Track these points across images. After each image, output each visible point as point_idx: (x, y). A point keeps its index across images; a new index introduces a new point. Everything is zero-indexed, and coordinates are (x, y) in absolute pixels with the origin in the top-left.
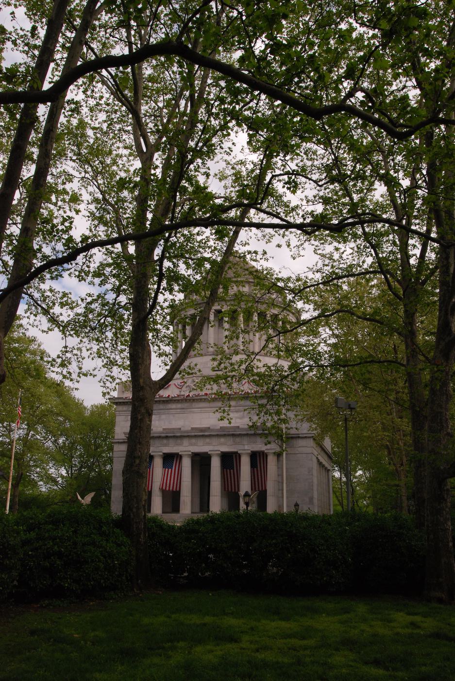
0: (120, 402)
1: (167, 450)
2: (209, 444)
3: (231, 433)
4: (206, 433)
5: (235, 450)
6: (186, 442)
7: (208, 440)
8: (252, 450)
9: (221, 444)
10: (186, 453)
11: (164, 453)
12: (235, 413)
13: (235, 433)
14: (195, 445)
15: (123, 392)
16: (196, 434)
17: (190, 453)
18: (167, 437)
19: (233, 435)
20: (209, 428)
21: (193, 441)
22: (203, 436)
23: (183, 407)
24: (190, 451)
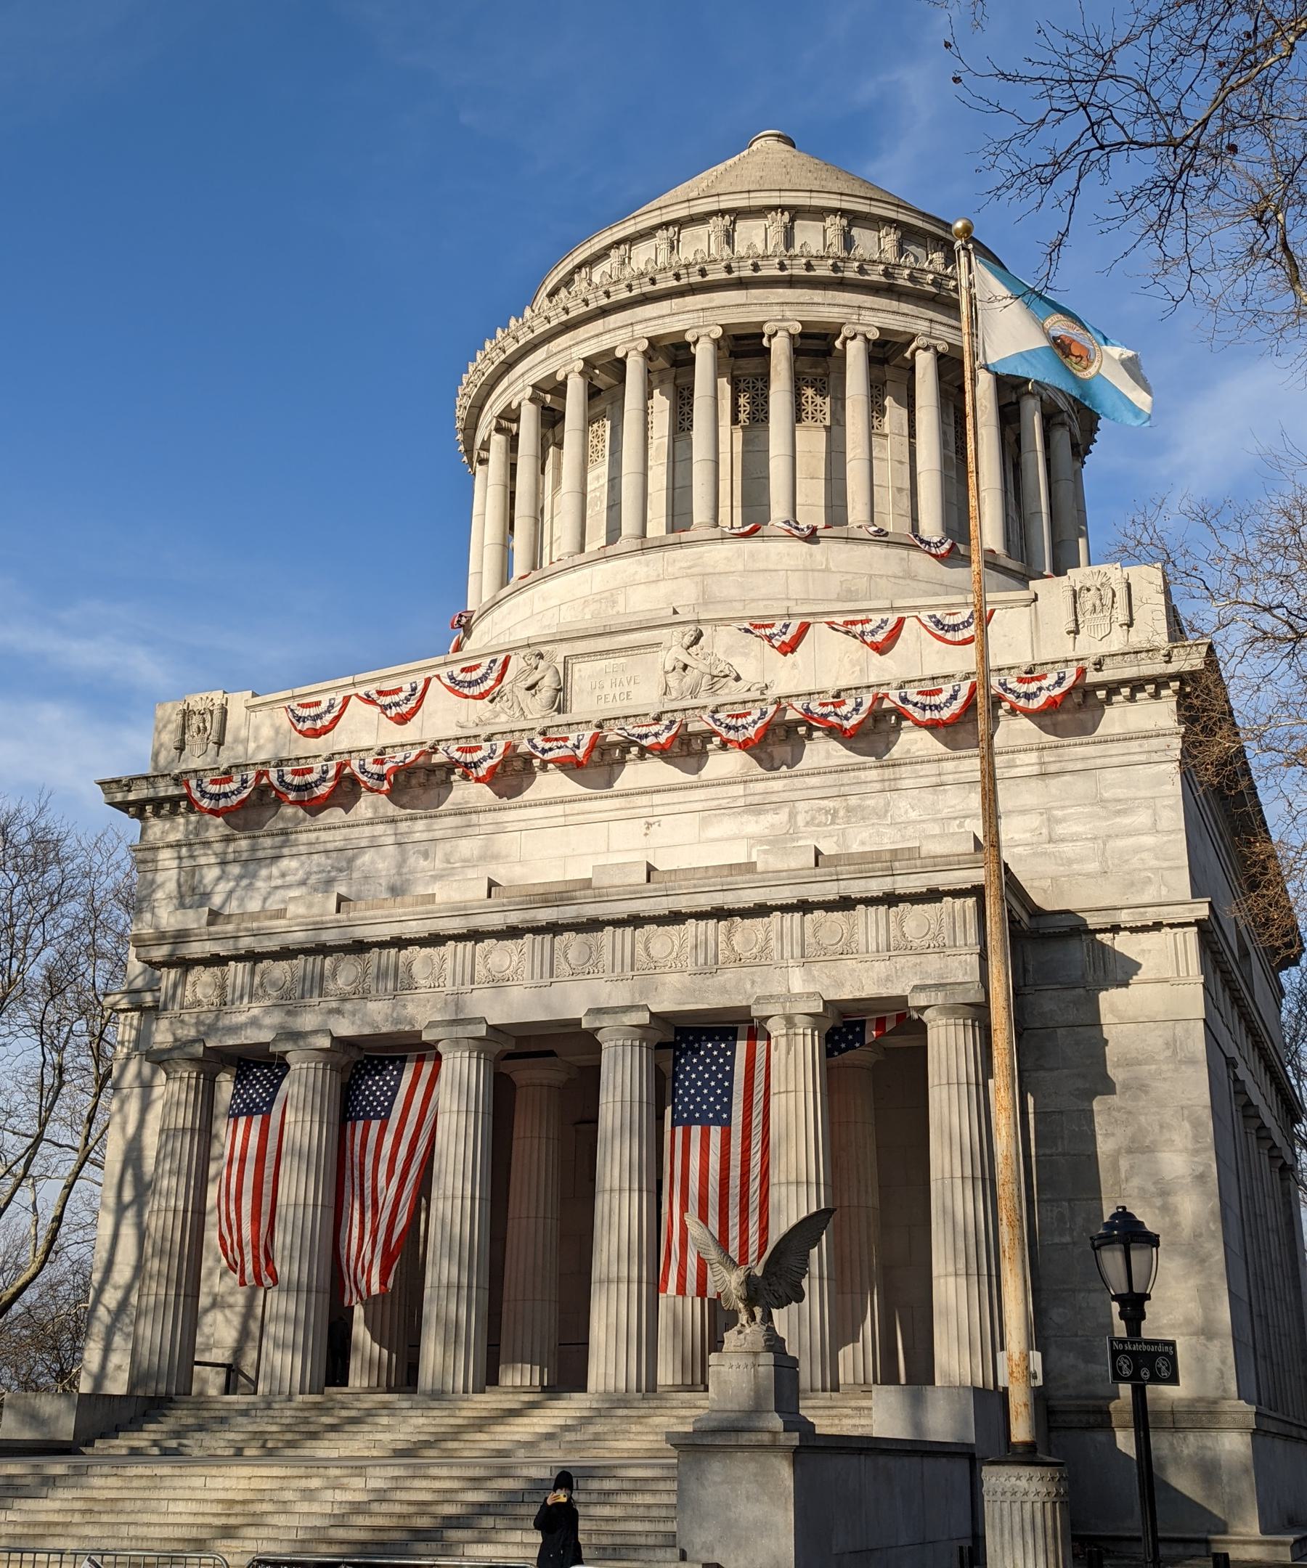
8: (833, 995)
17: (482, 1031)
20: (587, 884)
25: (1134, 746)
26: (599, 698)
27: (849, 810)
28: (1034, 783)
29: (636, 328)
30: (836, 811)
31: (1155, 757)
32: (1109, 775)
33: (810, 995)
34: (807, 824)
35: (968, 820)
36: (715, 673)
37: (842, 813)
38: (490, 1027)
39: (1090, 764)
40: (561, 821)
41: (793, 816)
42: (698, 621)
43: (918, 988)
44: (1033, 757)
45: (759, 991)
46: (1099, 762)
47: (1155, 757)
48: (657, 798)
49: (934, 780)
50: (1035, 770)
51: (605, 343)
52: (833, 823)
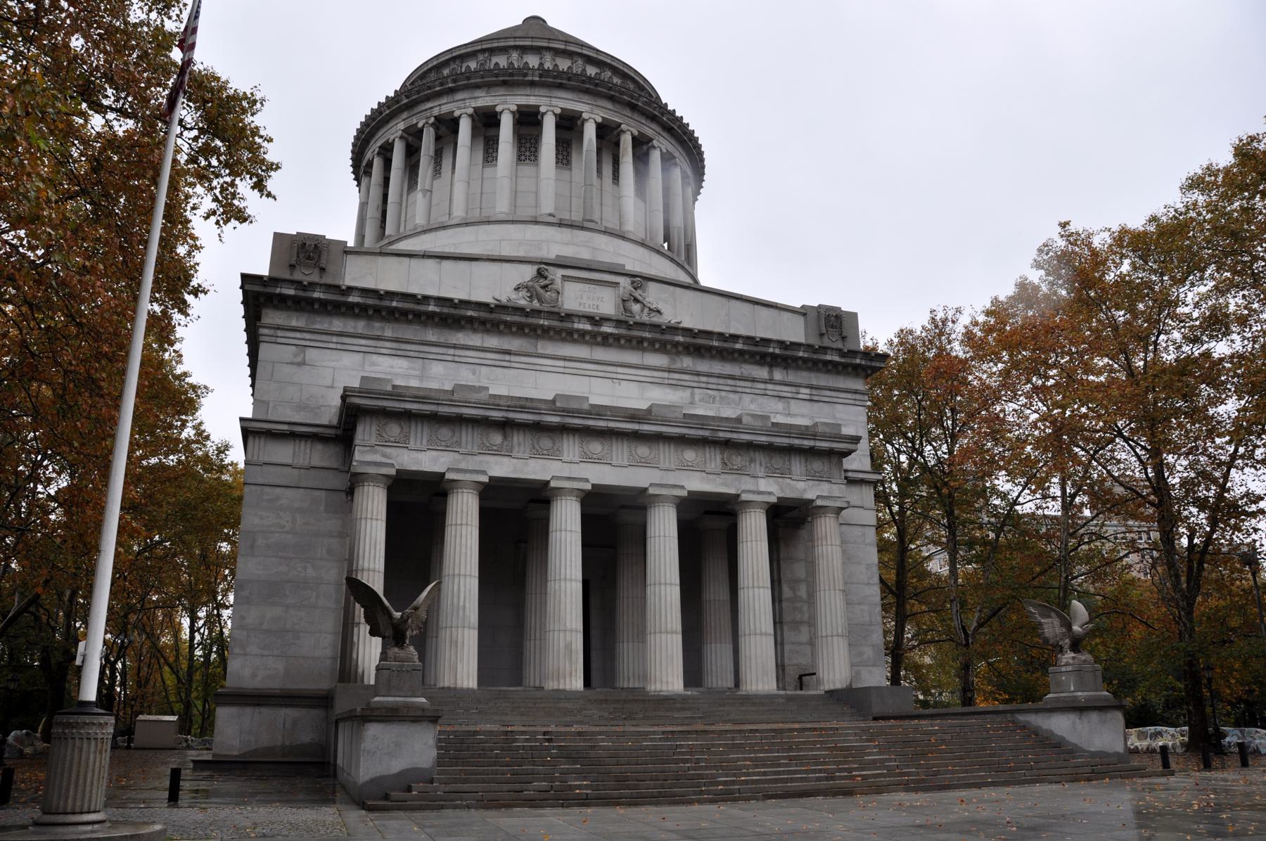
0: (283, 299)
1: (502, 468)
2: (644, 463)
3: (721, 434)
4: (646, 428)
5: (732, 491)
6: (571, 448)
7: (643, 450)
9: (686, 468)
10: (576, 485)
11: (491, 478)
12: (668, 390)
13: (735, 436)
14: (599, 461)
15: (292, 267)
16: (612, 425)
18: (505, 426)
19: (727, 444)
21: (596, 447)
22: (637, 437)
23: (506, 346)
24: (587, 480)
25: (849, 396)
26: (580, 304)
27: (721, 397)
28: (807, 403)
29: (552, 99)
30: (714, 398)
31: (857, 403)
32: (837, 406)
33: (770, 493)
34: (700, 401)
35: (778, 415)
36: (652, 307)
37: (718, 399)
38: (593, 485)
39: (830, 400)
40: (562, 370)
41: (693, 395)
42: (641, 277)
43: (818, 497)
44: (807, 391)
45: (744, 487)
46: (835, 400)
47: (857, 403)
48: (620, 370)
49: (762, 392)
50: (808, 397)
51: (532, 101)
52: (713, 403)
